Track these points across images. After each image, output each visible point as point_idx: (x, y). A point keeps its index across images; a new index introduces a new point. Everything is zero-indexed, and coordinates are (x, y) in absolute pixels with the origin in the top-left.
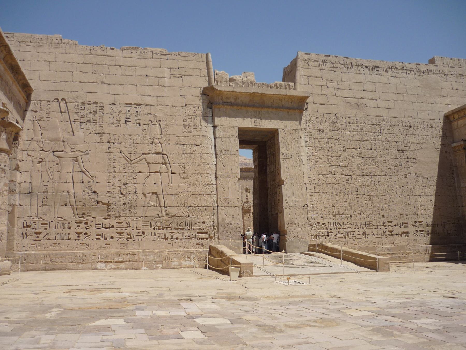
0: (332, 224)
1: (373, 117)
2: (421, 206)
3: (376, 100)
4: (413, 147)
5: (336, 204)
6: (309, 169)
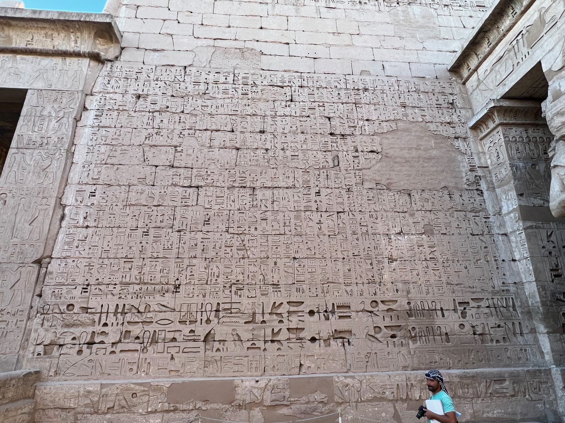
0: (112, 309)
1: (276, 73)
2: (391, 260)
3: (288, 44)
4: (369, 128)
5: (137, 256)
6: (86, 174)
